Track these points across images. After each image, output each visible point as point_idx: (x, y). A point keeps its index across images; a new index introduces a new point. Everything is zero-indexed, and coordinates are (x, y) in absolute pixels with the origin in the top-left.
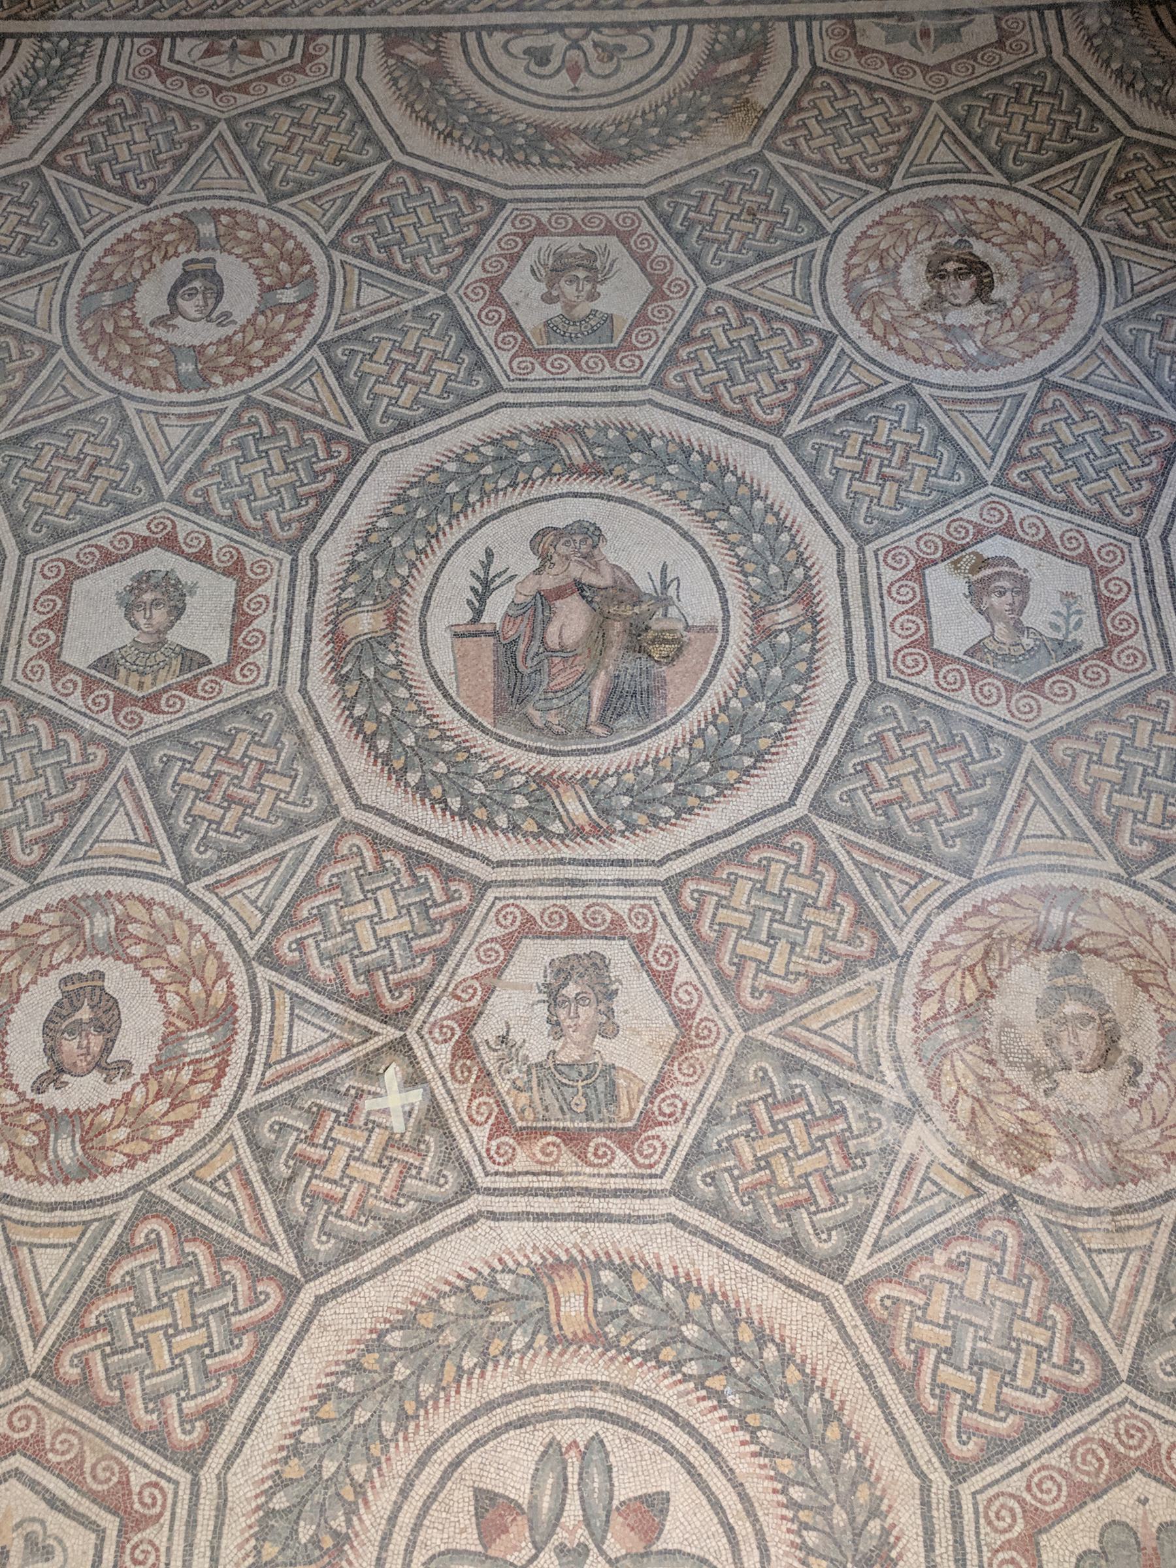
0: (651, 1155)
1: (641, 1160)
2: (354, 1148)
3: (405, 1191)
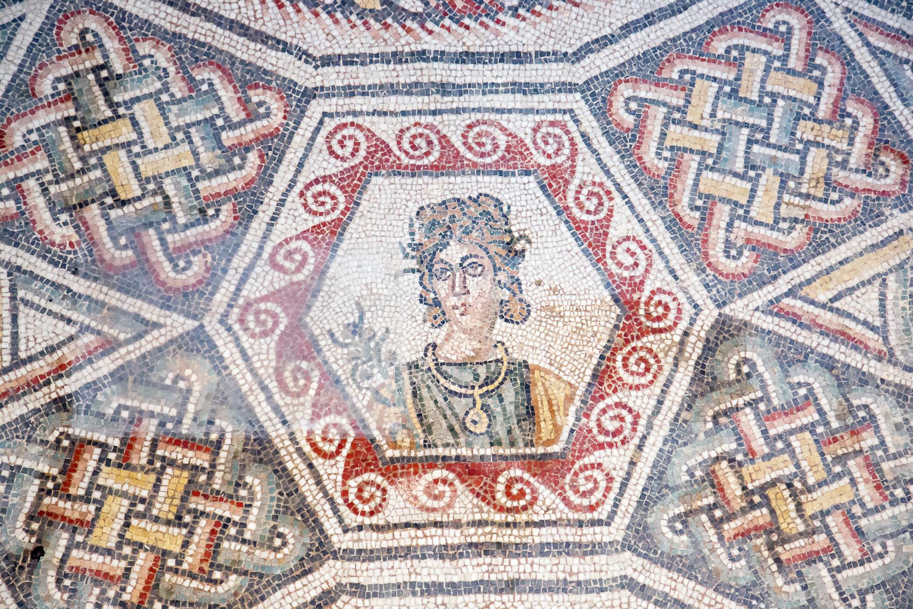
0: (591, 492)
1: (575, 499)
2: (135, 500)
3: (221, 560)
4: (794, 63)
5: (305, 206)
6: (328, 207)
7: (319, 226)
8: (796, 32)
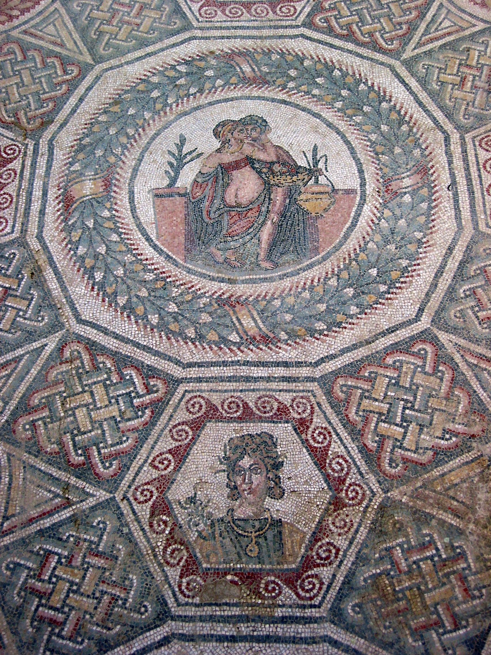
0: (311, 590)
2: (72, 583)
4: (428, 369)
5: (172, 437)
6: (183, 437)
7: (178, 447)
8: (429, 354)
